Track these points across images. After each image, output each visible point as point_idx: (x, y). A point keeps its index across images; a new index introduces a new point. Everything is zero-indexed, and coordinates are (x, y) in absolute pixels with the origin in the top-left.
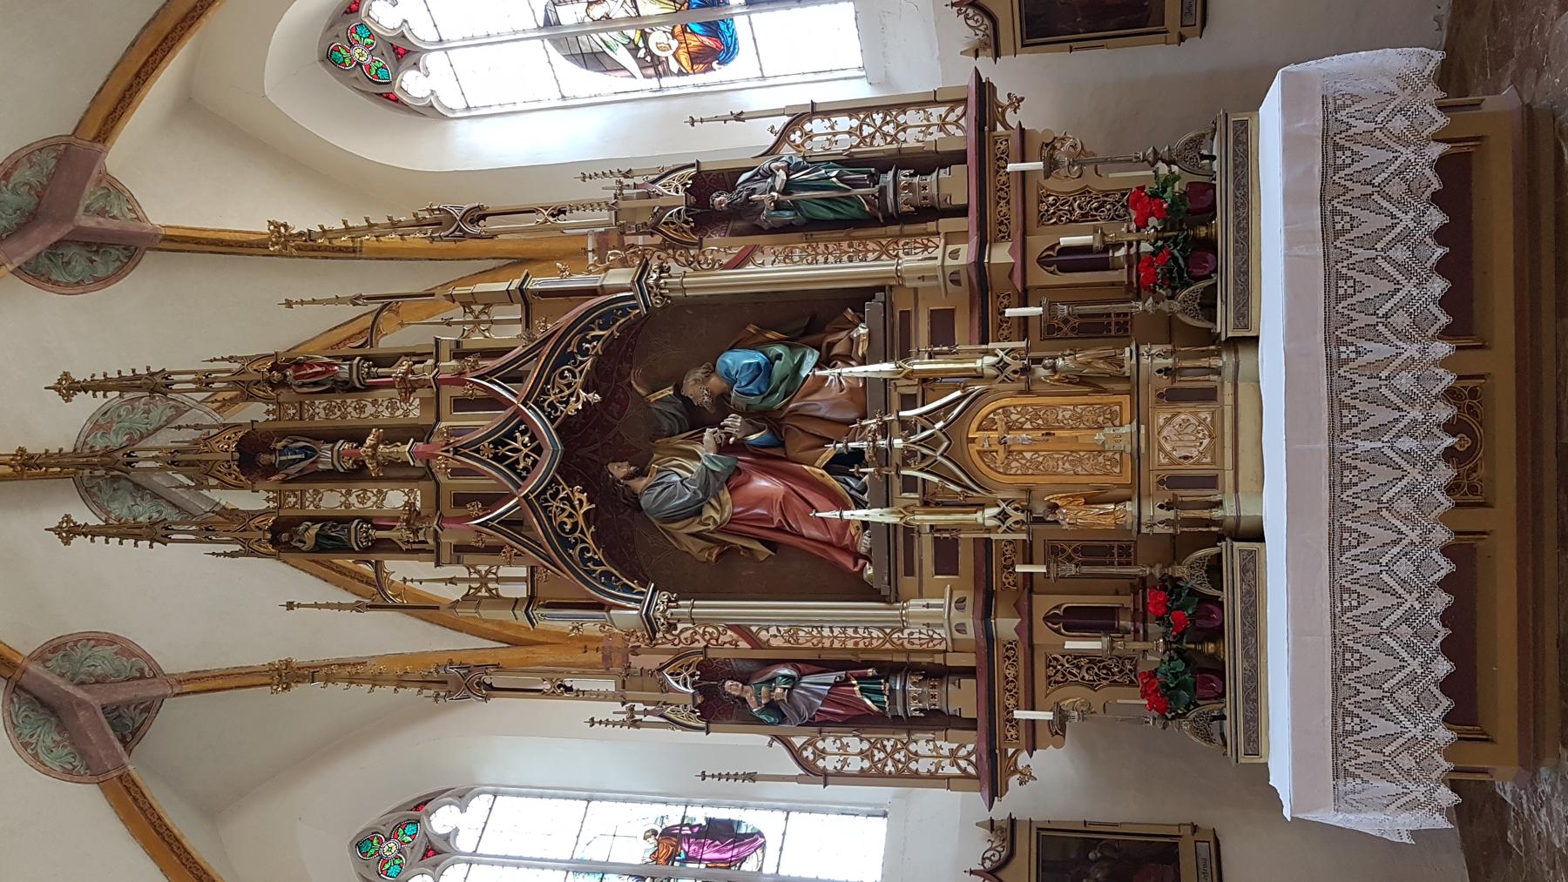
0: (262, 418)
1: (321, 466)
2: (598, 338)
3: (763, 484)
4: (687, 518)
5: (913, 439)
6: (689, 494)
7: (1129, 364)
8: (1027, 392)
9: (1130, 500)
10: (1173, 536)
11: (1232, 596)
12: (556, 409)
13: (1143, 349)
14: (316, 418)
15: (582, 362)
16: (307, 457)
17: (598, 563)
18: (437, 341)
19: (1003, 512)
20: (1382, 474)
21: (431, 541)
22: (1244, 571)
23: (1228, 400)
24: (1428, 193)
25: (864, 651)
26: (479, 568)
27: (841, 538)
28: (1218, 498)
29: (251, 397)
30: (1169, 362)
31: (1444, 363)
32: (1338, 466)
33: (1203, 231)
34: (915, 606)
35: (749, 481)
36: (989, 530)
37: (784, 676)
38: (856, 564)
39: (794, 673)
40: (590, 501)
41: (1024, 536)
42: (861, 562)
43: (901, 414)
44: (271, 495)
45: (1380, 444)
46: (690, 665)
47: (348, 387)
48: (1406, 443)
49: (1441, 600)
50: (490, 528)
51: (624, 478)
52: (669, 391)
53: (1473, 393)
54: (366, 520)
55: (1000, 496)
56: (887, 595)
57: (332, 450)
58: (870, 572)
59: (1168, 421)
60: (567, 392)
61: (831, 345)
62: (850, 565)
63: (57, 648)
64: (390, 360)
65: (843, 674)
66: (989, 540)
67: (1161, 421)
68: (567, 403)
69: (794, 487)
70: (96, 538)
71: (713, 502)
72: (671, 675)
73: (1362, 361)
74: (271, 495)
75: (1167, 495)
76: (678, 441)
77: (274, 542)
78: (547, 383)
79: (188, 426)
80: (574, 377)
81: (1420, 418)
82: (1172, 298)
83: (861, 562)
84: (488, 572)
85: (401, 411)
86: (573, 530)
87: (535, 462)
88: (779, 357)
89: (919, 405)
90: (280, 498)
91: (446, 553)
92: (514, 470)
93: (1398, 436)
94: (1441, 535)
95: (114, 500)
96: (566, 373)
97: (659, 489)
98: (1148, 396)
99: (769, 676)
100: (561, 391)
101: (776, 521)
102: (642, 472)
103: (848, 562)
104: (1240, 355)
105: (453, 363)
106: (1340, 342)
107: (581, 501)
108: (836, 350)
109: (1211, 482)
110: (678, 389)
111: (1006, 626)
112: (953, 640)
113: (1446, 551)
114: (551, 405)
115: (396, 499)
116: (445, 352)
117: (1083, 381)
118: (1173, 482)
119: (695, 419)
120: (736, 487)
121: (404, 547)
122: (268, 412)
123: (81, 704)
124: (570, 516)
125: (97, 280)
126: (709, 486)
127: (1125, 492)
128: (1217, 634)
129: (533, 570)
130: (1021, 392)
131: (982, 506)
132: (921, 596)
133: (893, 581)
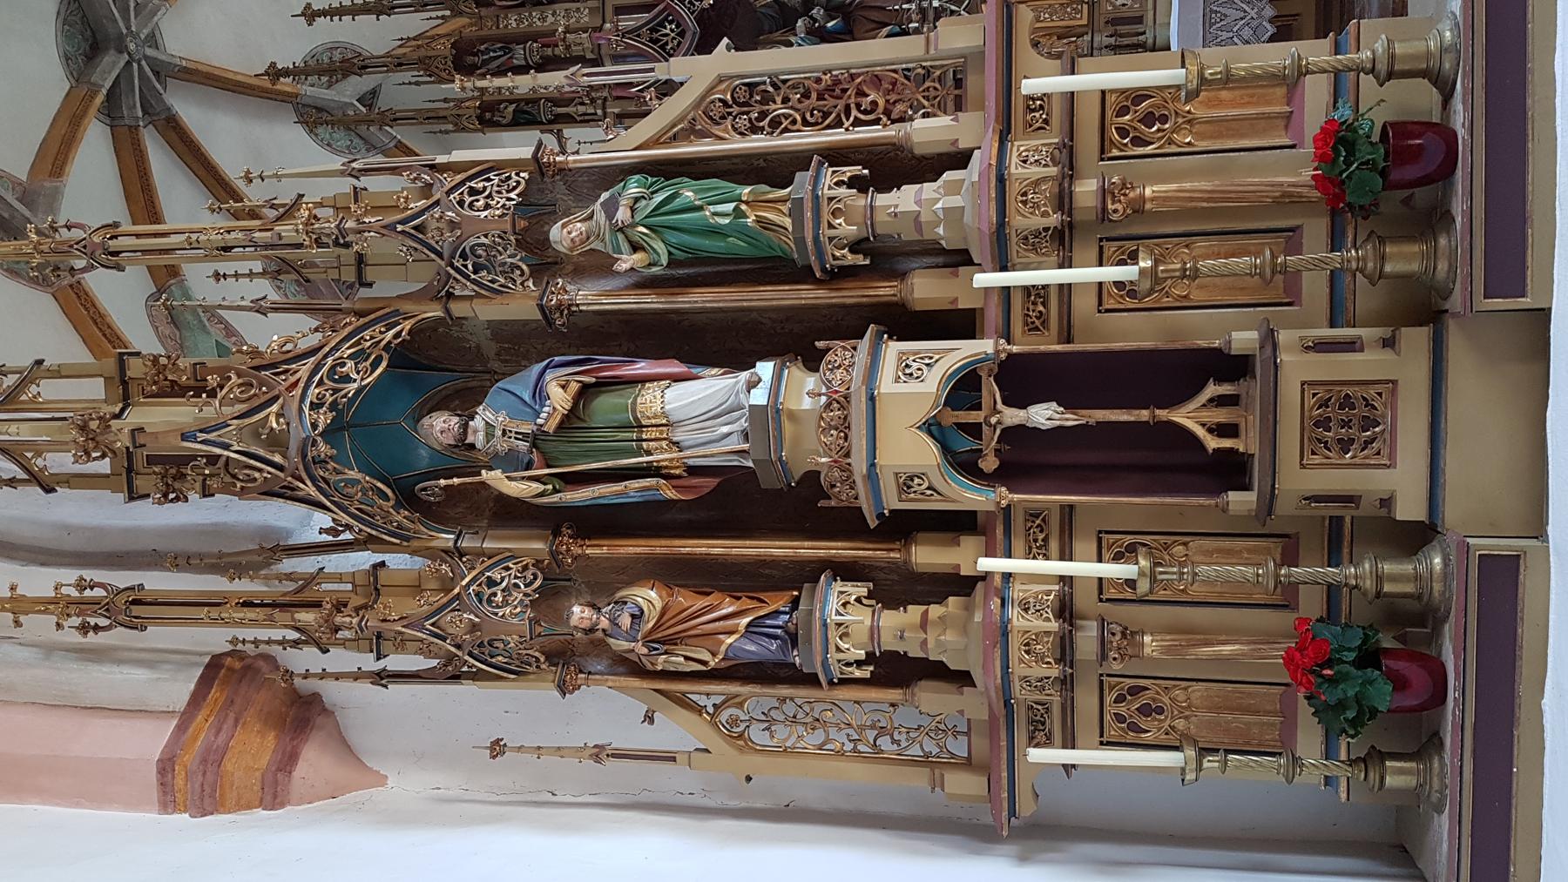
16: (505, 54)
54: (548, 100)
57: (524, 49)
77: (481, 119)
85: (574, 19)
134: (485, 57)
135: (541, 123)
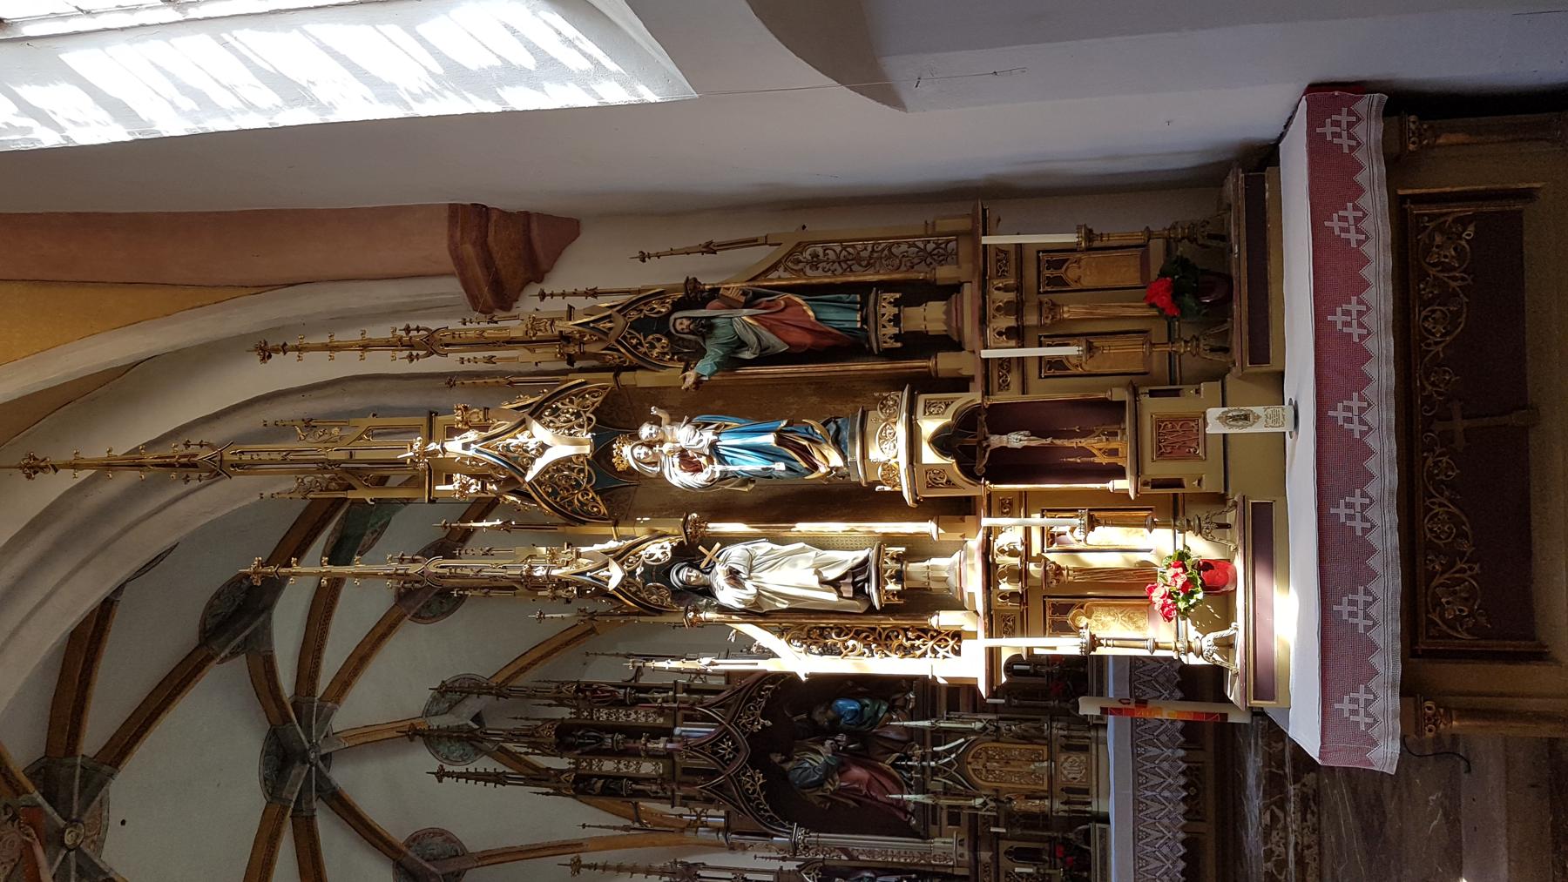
0: (567, 716)
1: (604, 747)
2: (769, 689)
3: (857, 772)
4: (814, 787)
5: (940, 762)
6: (818, 776)
7: (1047, 733)
8: (997, 741)
9: (1047, 798)
10: (1069, 818)
11: (1095, 850)
12: (746, 727)
13: (1054, 725)
14: (601, 719)
15: (760, 702)
17: (766, 811)
18: (676, 682)
19: (985, 802)
20: (1155, 807)
21: (669, 793)
22: (1101, 837)
23: (1094, 752)
24: (1175, 682)
25: (910, 864)
26: (697, 809)
27: (901, 806)
28: (1089, 800)
29: (561, 703)
30: (1066, 733)
31: (1182, 759)
32: (1137, 802)
33: (1082, 670)
34: (938, 842)
35: (849, 769)
36: (977, 809)
37: (867, 877)
38: (906, 817)
39: (872, 875)
40: (763, 778)
41: (995, 814)
42: (909, 816)
43: (935, 749)
44: (572, 761)
45: (1154, 793)
46: (815, 868)
47: (621, 704)
48: (1166, 793)
49: (1182, 865)
50: (708, 790)
51: (779, 763)
52: (804, 716)
53: (1198, 769)
54: (629, 778)
55: (983, 792)
56: (925, 837)
58: (914, 822)
59: (1066, 760)
60: (752, 719)
61: (895, 700)
62: (903, 818)
63: (415, 839)
64: (647, 689)
65: (899, 877)
66: (977, 814)
67: (1063, 760)
68: (752, 724)
69: (873, 774)
70: (459, 780)
71: (830, 780)
72: (806, 874)
73: (1147, 755)
74: (572, 761)
75: (1065, 796)
76: (808, 743)
78: (741, 713)
79: (521, 718)
80: (756, 710)
81: (1172, 782)
82: (1067, 701)
83: (909, 816)
84: (701, 812)
86: (753, 793)
87: (734, 756)
88: (867, 705)
89: (943, 743)
90: (577, 764)
91: (678, 801)
92: (722, 761)
93: (1163, 790)
94: (1181, 836)
95: (439, 744)
96: (752, 708)
97: (800, 771)
98: (1056, 747)
99: (859, 877)
100: (749, 718)
101: (864, 792)
102: (789, 759)
103: (902, 816)
104: (1099, 733)
105: (684, 695)
106: (1138, 746)
107: (759, 779)
108: (897, 704)
109: (1086, 792)
110: (809, 716)
111: (985, 856)
112: (957, 861)
113: (1183, 842)
114: (743, 725)
115: (647, 768)
116: (680, 688)
117: (1025, 738)
118: (1069, 790)
119: (821, 733)
120: (844, 772)
121: (652, 795)
122: (571, 713)
123: (432, 874)
124: (752, 785)
125: (443, 613)
126: (829, 771)
127: (1046, 794)
128: (1088, 869)
129: (728, 813)
130: (993, 741)
131: (975, 797)
132: (940, 836)
133: (926, 829)
134: (581, 741)
135: (623, 796)
